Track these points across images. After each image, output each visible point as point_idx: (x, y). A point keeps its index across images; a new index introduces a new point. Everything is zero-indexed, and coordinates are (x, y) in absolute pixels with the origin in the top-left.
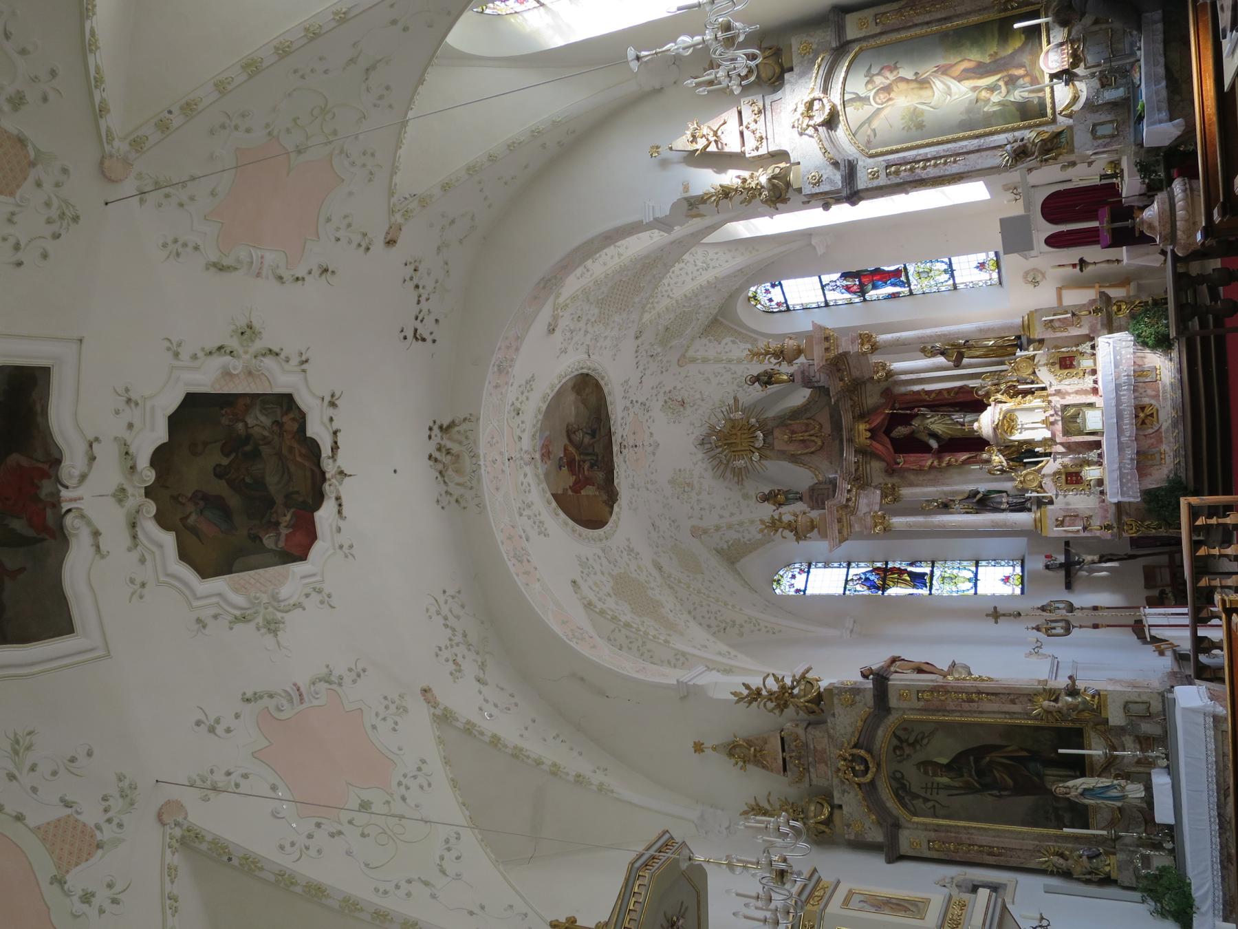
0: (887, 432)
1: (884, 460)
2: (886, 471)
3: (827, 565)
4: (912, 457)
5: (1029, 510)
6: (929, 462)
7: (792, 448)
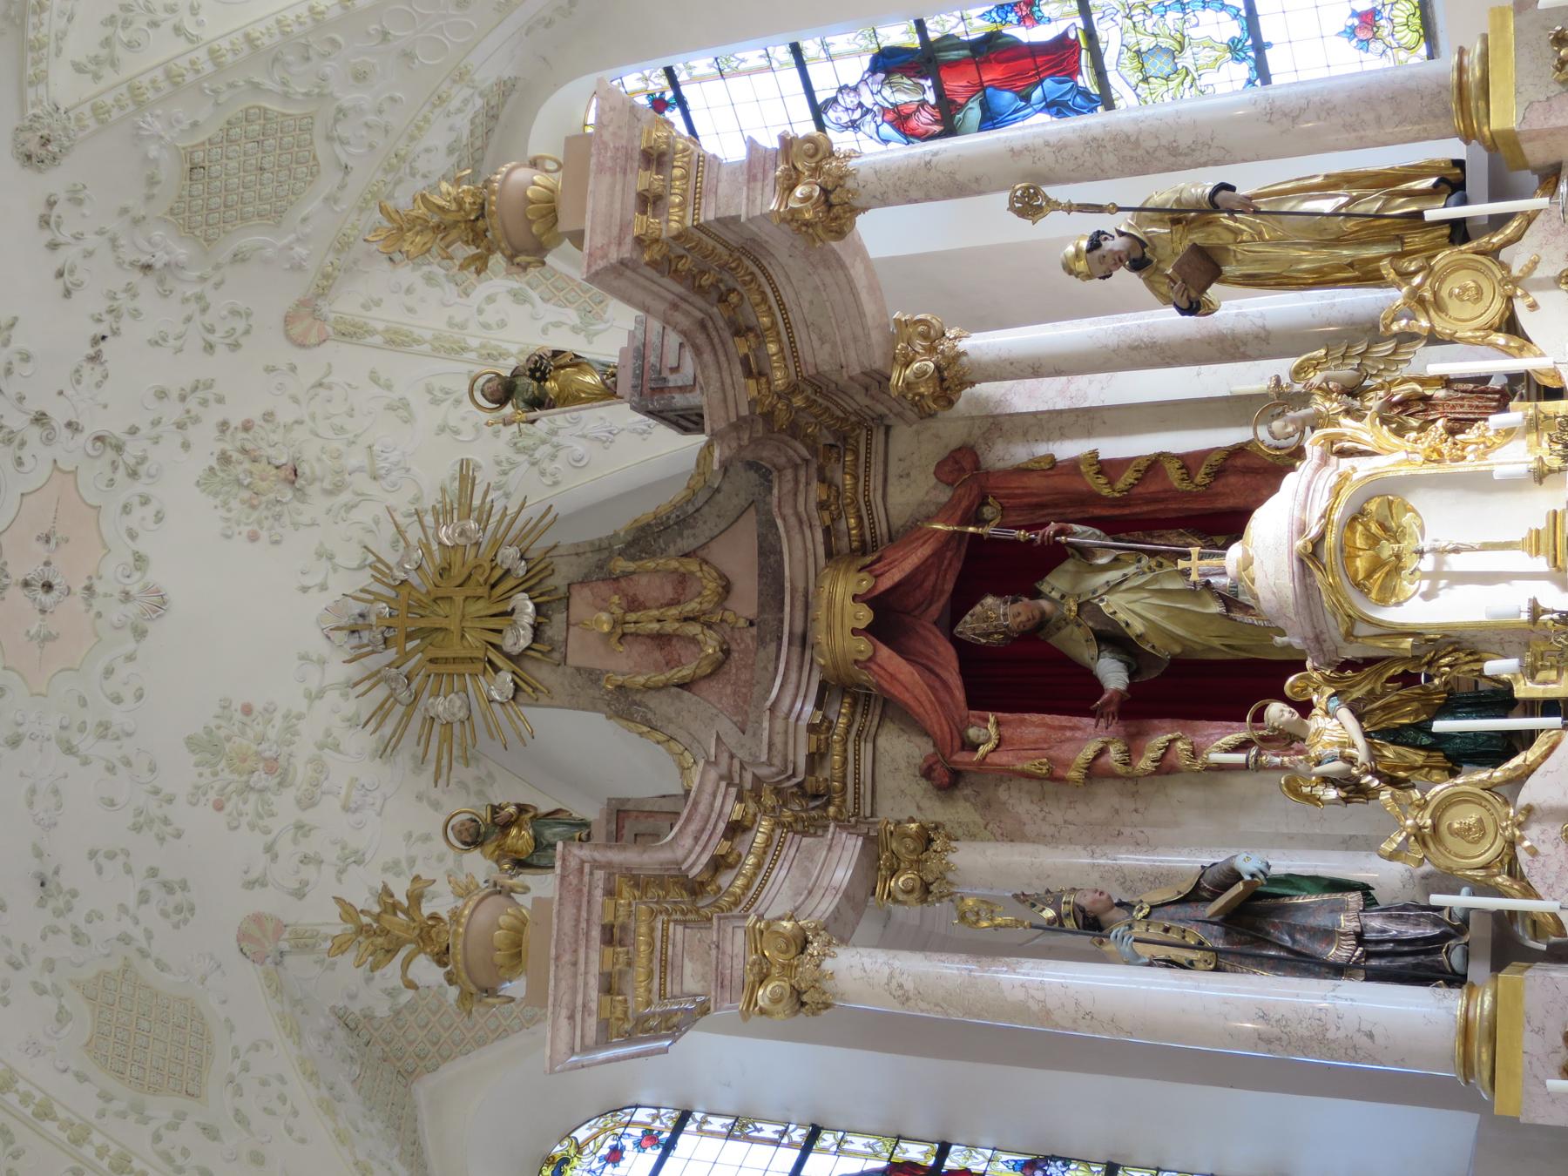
1: (926, 733)
2: (927, 773)
3: (739, 1129)
4: (1034, 726)
5: (1456, 980)
6: (1089, 751)
7: (627, 665)
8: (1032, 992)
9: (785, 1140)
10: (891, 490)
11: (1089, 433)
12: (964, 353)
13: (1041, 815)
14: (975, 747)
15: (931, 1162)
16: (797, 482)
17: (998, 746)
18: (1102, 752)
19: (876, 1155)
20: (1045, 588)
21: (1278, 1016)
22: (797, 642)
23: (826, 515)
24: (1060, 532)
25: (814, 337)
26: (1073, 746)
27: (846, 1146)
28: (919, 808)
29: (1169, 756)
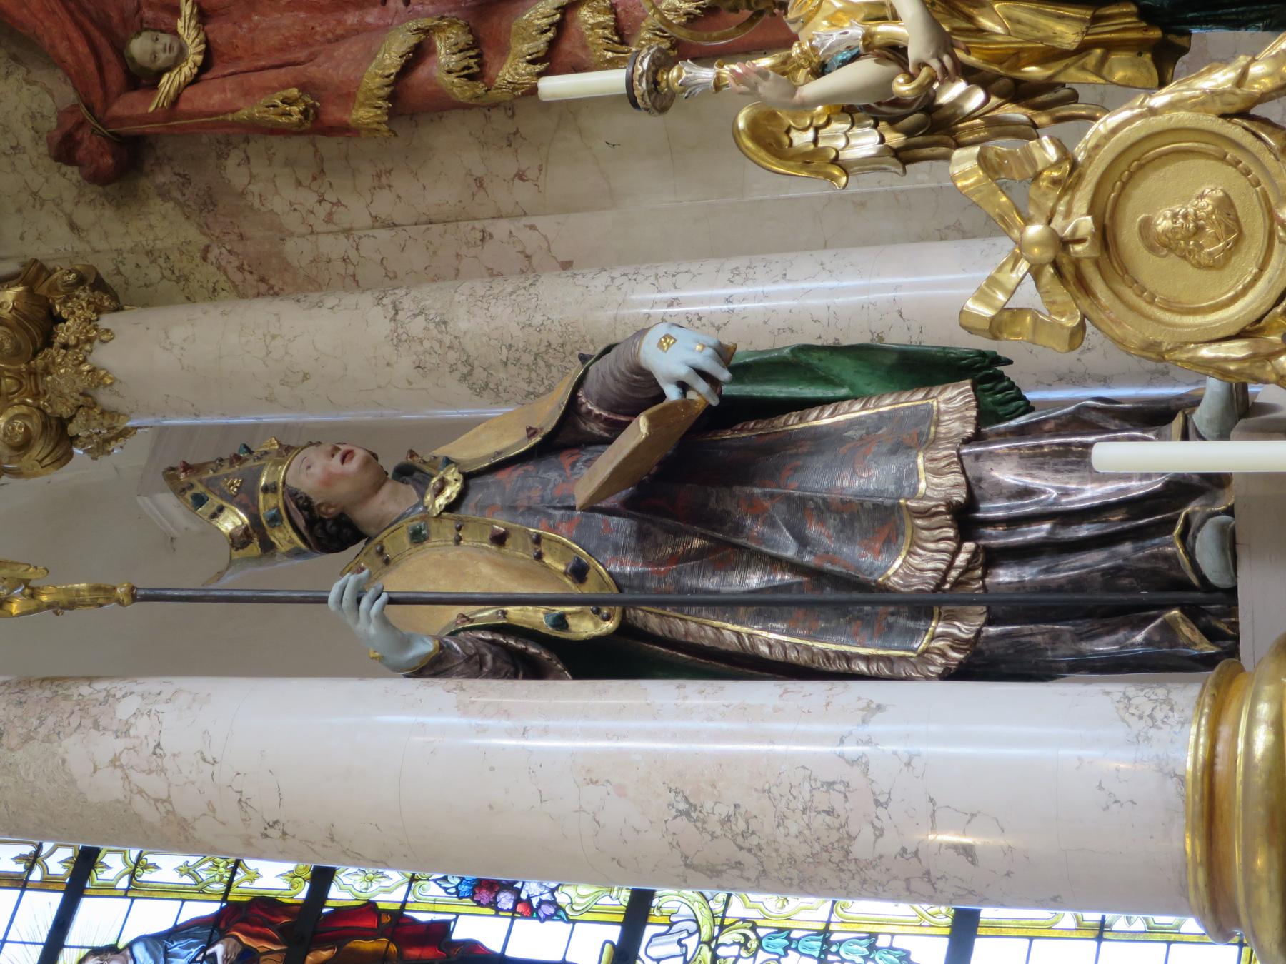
1: (53, 61)
2: (65, 150)
6: (391, 56)
8: (138, 778)
9: (36, 875)
13: (322, 211)
14: (144, 79)
15: (302, 894)
17: (204, 67)
18: (419, 53)
19: (200, 891)
21: (723, 810)
26: (353, 47)
27: (146, 877)
28: (73, 227)
29: (566, 46)
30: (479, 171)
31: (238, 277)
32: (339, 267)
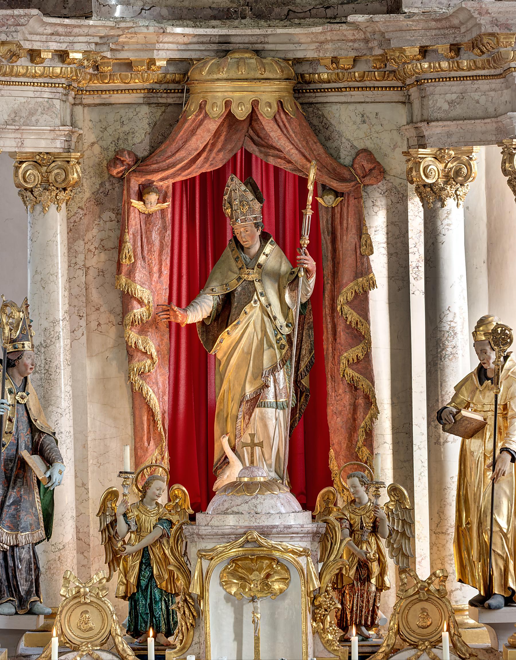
0: (243, 165)
10: (352, 107)
11: (391, 278)
12: (443, 205)
13: (92, 248)
14: (141, 197)
16: (354, 41)
18: (141, 302)
20: (268, 248)
22: (222, 40)
23: (329, 61)
24: (307, 271)
25: (454, 96)
28: (93, 144)
30: (102, 310)
31: (72, 220)
32: (73, 261)
